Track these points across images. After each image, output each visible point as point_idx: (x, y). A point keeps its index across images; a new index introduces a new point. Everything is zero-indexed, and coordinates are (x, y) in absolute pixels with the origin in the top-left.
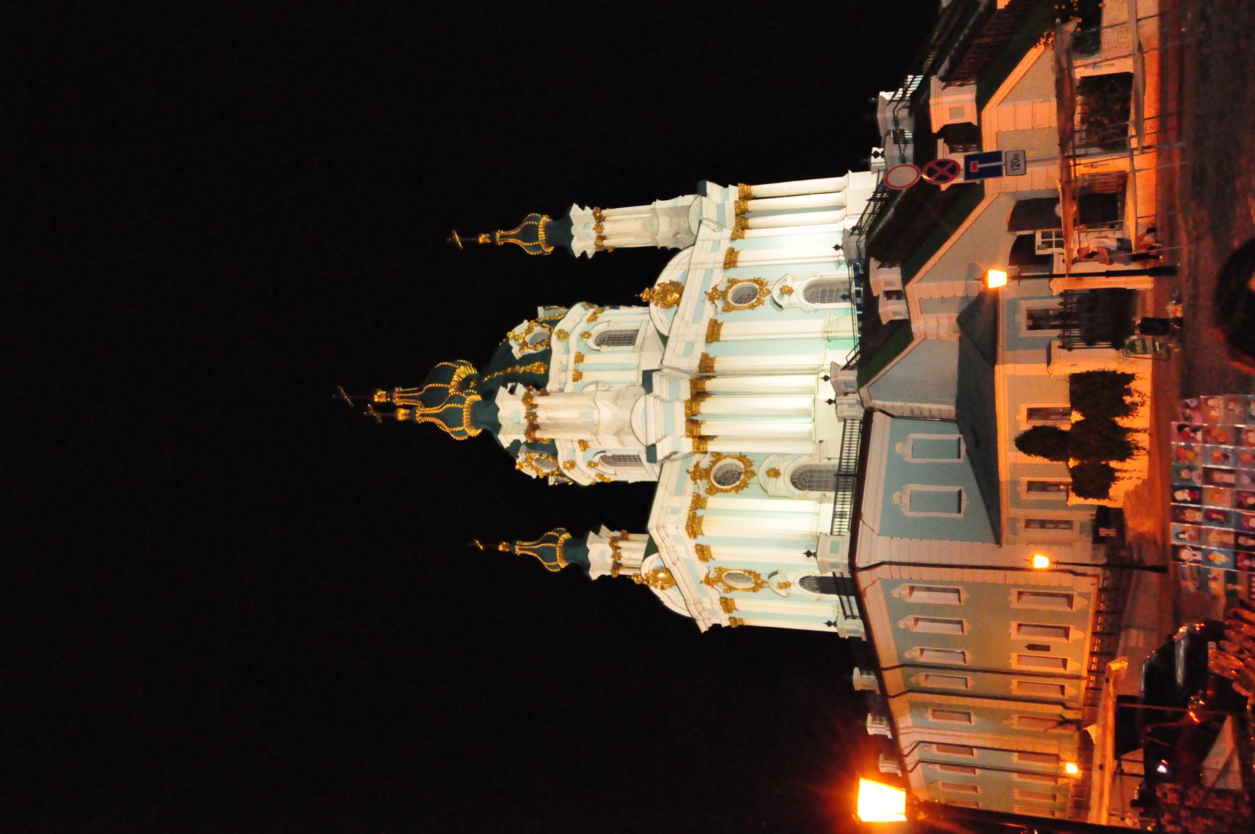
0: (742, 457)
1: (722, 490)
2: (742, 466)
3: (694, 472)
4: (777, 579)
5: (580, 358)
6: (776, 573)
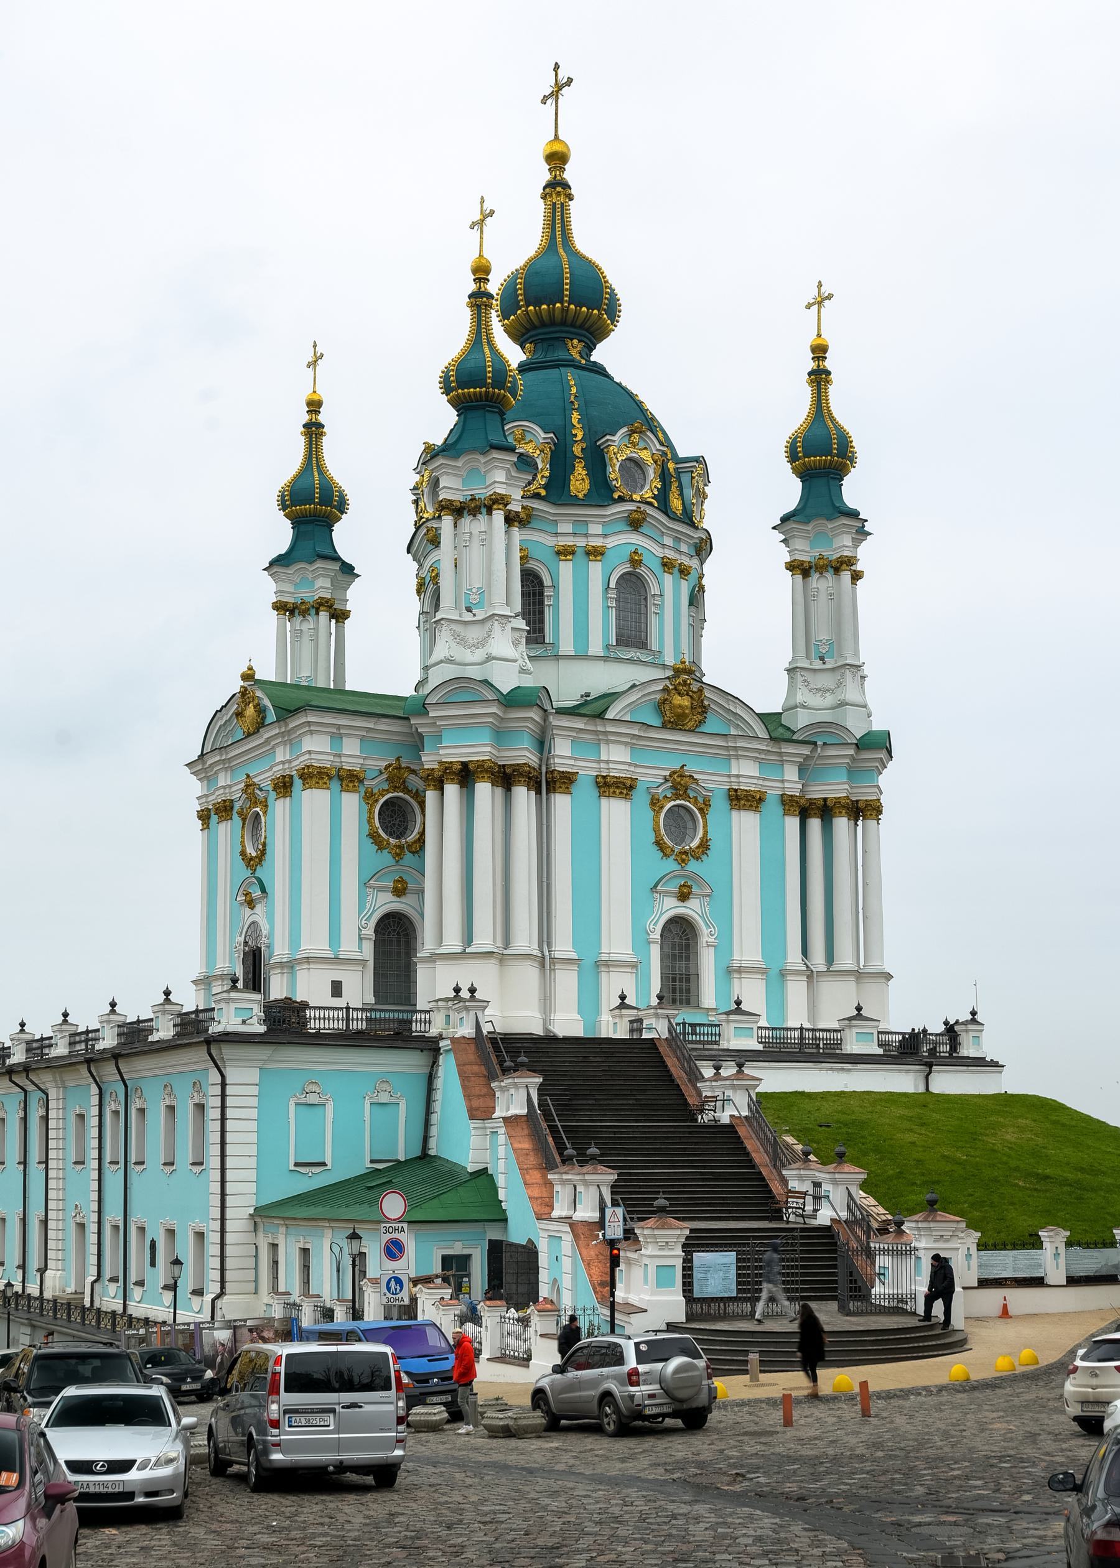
0: (421, 839)
2: (413, 836)
3: (399, 768)
4: (256, 893)
5: (595, 553)
6: (263, 890)
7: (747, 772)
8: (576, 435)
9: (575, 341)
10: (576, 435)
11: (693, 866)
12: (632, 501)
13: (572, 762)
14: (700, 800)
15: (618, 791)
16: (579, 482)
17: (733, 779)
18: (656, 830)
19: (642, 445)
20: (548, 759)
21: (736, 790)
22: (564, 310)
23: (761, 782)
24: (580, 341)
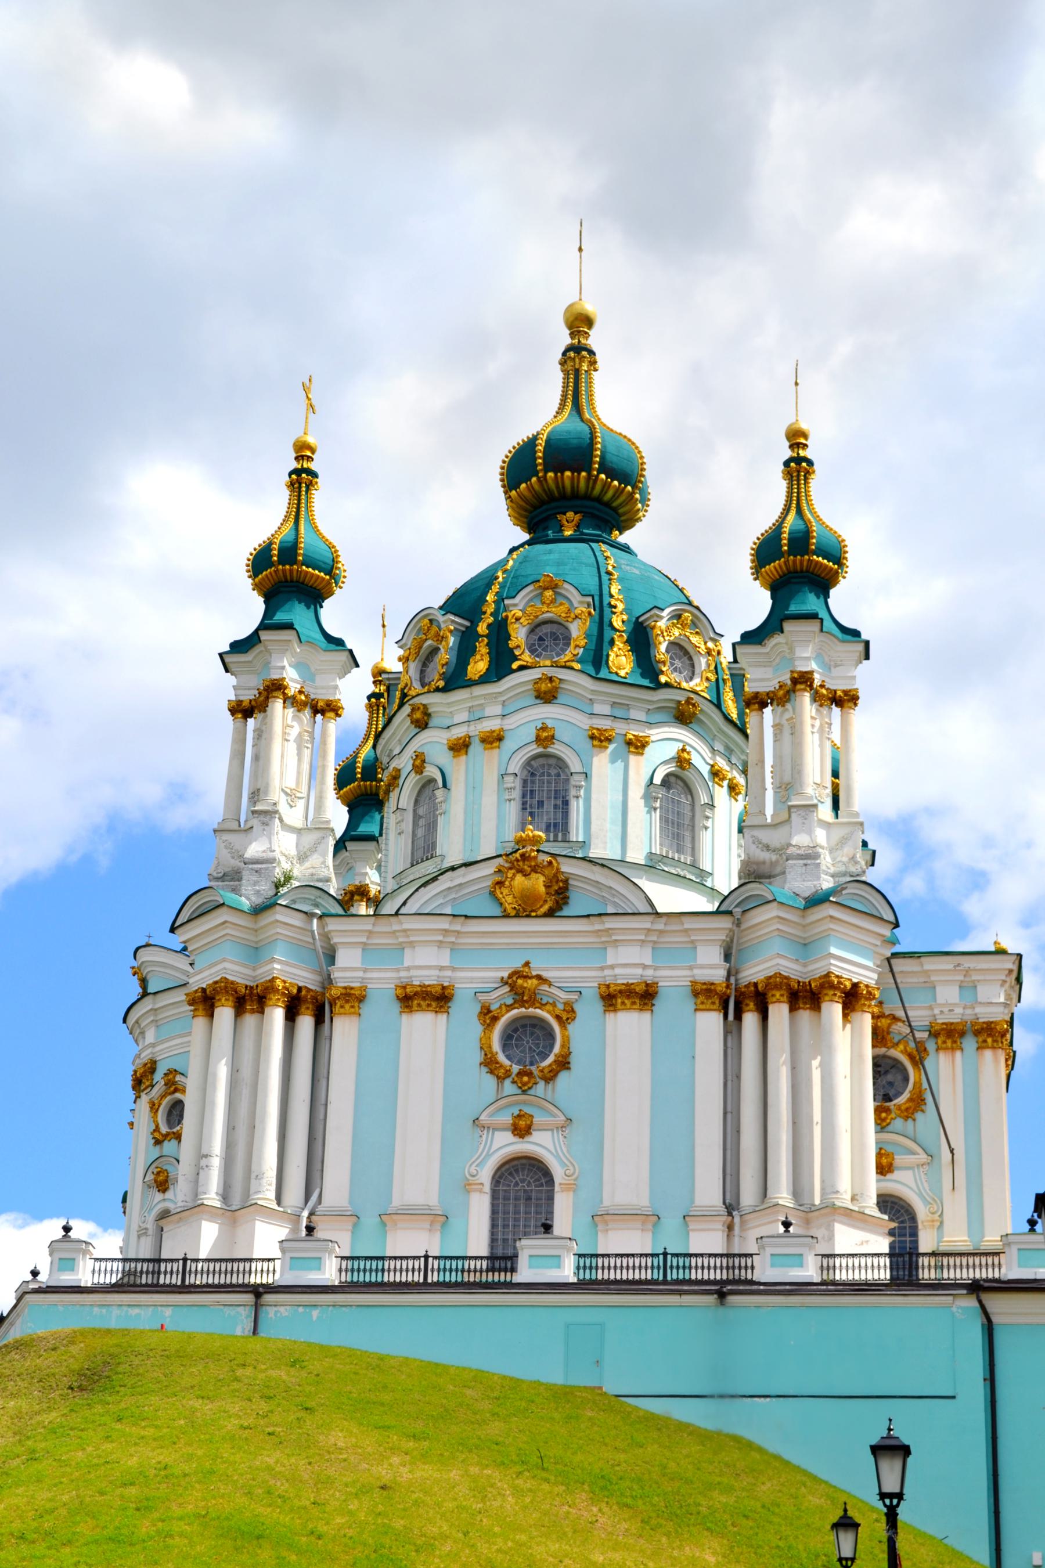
7: (629, 962)
9: (570, 514)
11: (540, 1088)
15: (422, 1003)
18: (485, 1048)
19: (560, 600)
21: (608, 986)
22: (542, 481)
24: (576, 513)
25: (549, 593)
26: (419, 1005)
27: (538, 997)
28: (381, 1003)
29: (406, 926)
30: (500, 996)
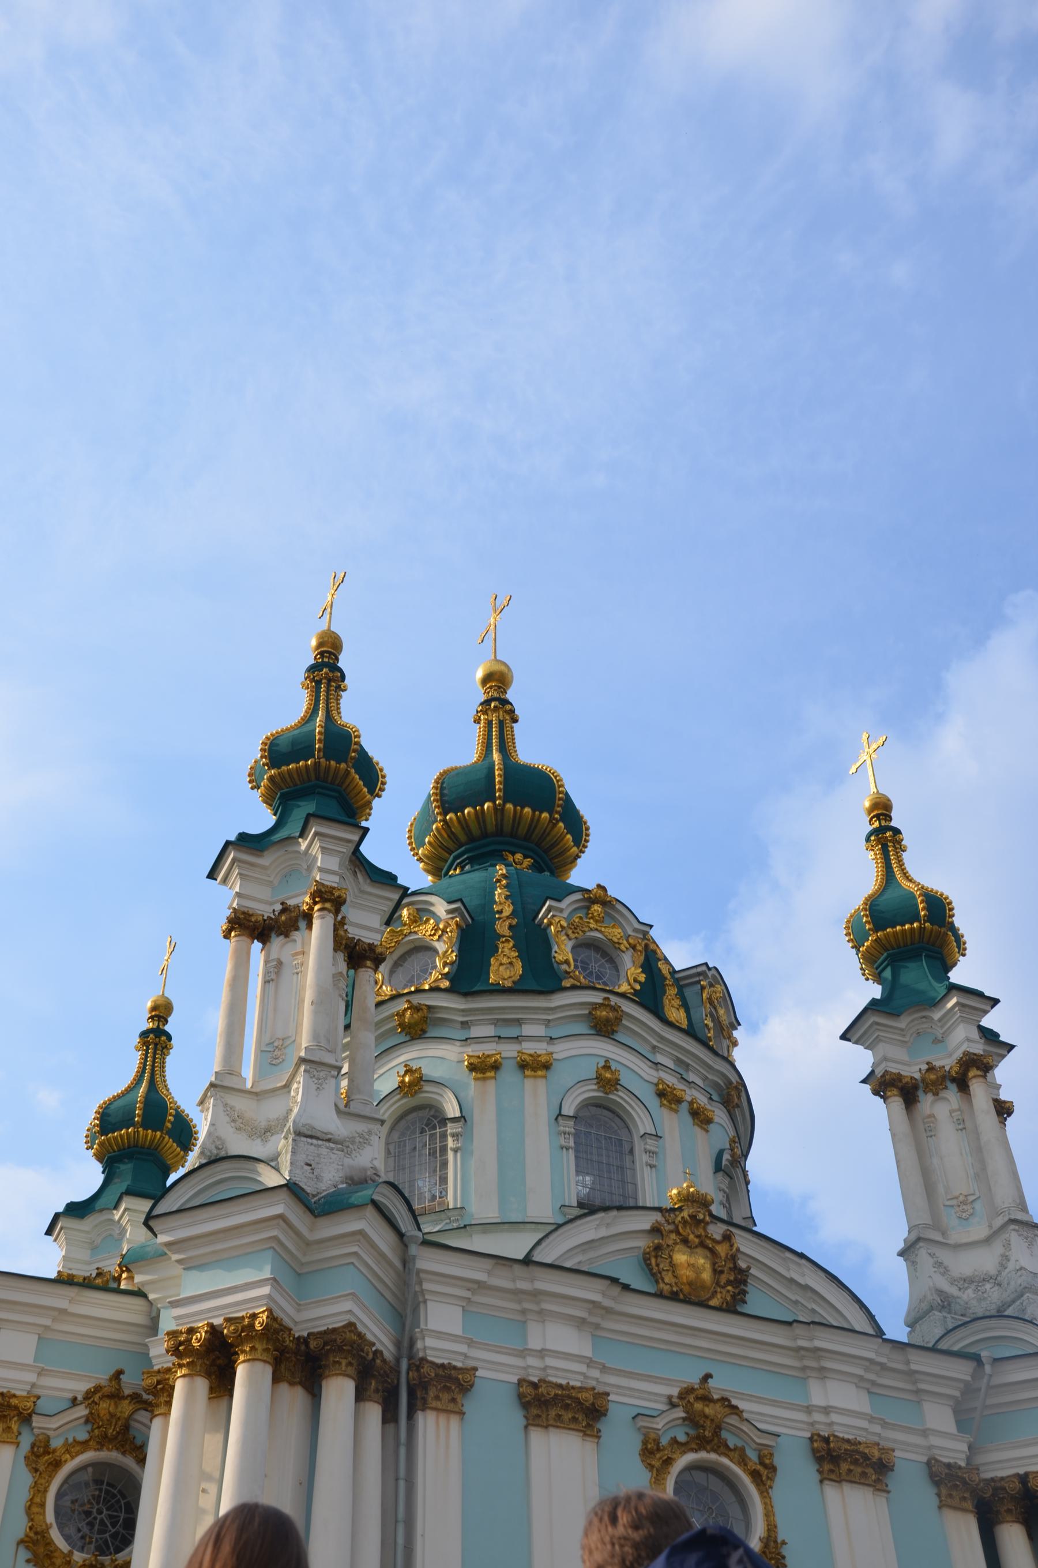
1: (39, 1490)
3: (116, 1396)
7: (844, 1405)
8: (500, 912)
9: (519, 856)
10: (500, 912)
12: (594, 989)
13: (463, 1348)
14: (752, 1455)
15: (567, 1416)
16: (505, 966)
17: (818, 1417)
20: (412, 1343)
21: (826, 1440)
22: (499, 811)
23: (877, 1429)
24: (525, 857)
25: (597, 908)
26: (559, 1416)
27: (724, 1434)
28: (493, 1406)
29: (540, 1285)
30: (669, 1425)
